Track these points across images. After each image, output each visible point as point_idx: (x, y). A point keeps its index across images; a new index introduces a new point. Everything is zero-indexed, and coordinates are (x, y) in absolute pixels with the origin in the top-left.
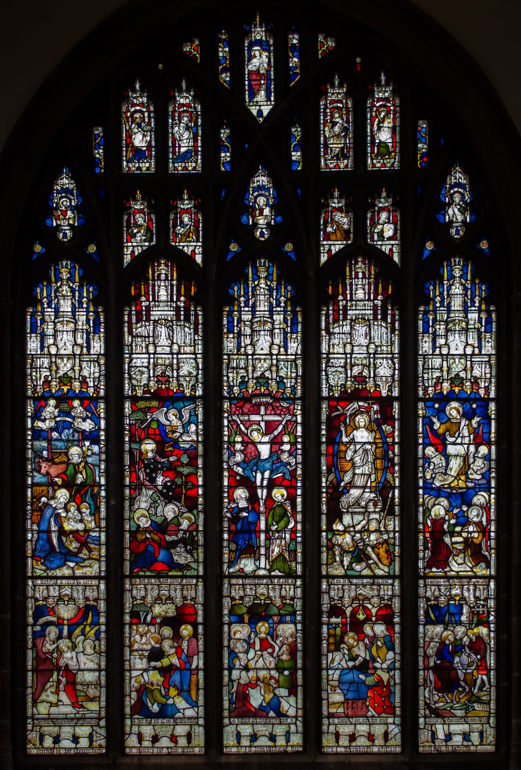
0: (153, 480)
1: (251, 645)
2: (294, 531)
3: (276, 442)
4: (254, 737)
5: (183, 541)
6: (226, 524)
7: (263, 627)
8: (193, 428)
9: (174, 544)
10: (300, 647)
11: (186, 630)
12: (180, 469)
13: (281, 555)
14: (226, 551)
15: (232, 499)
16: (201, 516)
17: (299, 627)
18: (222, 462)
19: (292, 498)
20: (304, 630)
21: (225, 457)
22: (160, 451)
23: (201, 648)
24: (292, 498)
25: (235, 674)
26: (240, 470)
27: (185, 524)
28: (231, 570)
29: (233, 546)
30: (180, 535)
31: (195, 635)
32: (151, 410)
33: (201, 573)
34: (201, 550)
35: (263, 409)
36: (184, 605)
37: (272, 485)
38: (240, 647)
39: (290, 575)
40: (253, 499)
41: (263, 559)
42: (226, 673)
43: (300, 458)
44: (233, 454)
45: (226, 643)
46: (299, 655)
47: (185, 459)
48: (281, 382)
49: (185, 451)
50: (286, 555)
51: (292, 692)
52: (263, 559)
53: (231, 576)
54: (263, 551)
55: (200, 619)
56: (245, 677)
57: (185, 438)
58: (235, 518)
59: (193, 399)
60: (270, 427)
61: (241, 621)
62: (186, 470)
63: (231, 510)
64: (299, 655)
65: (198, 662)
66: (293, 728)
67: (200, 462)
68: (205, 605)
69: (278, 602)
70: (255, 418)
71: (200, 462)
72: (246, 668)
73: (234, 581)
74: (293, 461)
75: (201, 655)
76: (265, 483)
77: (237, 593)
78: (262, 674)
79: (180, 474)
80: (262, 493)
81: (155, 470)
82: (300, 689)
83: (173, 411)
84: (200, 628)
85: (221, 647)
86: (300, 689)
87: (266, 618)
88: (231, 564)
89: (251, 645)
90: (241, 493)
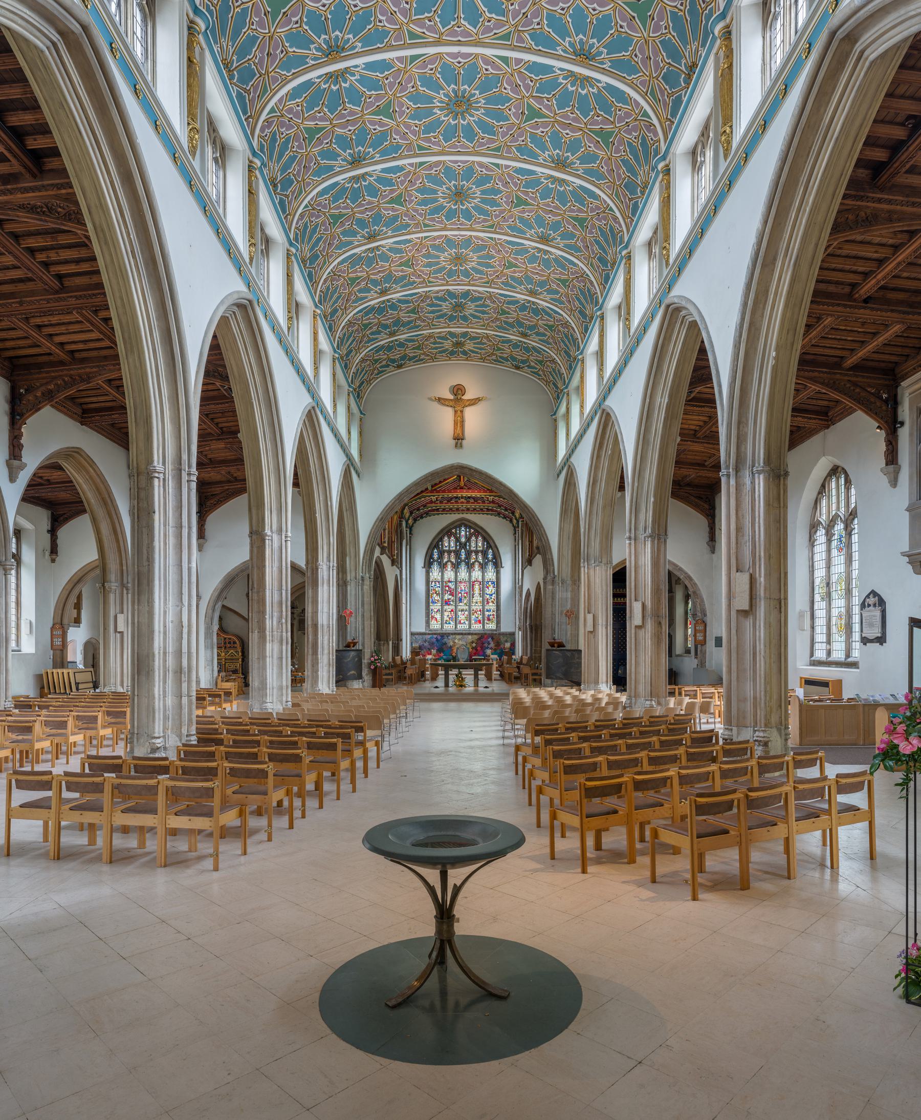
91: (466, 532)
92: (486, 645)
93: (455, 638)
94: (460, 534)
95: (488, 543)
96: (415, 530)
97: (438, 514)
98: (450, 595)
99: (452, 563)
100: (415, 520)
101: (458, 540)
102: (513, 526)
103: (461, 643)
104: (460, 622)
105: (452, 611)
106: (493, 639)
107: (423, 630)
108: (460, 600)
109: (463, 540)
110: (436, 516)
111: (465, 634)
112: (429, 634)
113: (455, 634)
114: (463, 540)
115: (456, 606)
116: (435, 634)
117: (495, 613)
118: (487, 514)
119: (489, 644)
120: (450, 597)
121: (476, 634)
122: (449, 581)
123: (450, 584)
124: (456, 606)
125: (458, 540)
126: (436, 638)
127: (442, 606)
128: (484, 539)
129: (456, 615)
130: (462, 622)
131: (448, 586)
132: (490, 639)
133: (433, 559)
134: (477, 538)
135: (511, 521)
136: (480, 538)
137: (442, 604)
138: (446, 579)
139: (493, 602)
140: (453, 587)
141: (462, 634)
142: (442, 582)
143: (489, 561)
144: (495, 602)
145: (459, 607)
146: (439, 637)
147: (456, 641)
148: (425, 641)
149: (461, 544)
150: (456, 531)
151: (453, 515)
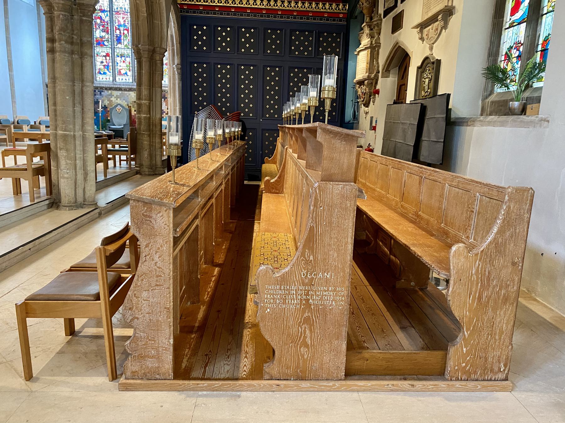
0: (99, 28)
1: (121, 62)
2: (129, 40)
3: (125, 21)
4: (122, 79)
5: (106, 40)
6: (115, 37)
7: (123, 58)
8: (107, 17)
9: (105, 41)
10: (131, 62)
12: (105, 26)
13: (126, 44)
14: (115, 43)
15: (116, 32)
16: (110, 36)
17: (131, 59)
18: (113, 25)
19: (128, 33)
20: (132, 59)
21: (114, 24)
22: (101, 22)
23: (111, 61)
24: (128, 33)
25: (118, 67)
26: (117, 27)
27: (107, 37)
28: (117, 46)
29: (117, 42)
30: (106, 39)
31: (110, 59)
32: (98, 13)
33: (110, 47)
34: (110, 42)
35: (121, 14)
36: (107, 53)
37: (124, 30)
38: (119, 62)
39: (128, 48)
40: (120, 33)
41: (123, 44)
42: (116, 67)
43: (130, 25)
44: (115, 23)
45: (116, 61)
46: (131, 64)
47: (106, 24)
48: (125, 9)
49: (106, 22)
50: (127, 44)
51: (130, 71)
52: (123, 44)
53: (116, 48)
54: (123, 43)
55: (111, 56)
56: (120, 68)
57: (106, 19)
58: (117, 37)
59: (107, 11)
60: (123, 18)
61: (119, 56)
62: (106, 26)
63: (116, 35)
64: (131, 64)
65: (111, 64)
66: (130, 78)
67: (109, 24)
68: (111, 53)
69: (126, 54)
70: (119, 16)
71: (109, 24)
72: (120, 66)
73: (117, 49)
74: (128, 25)
75: (111, 63)
76: (123, 30)
77: (118, 51)
78: (124, 67)
79: (105, 27)
80: (122, 32)
81: (100, 26)
82: (131, 71)
83: (103, 14)
84: (111, 58)
85: (115, 62)
86: (131, 71)
87: (124, 56)
88: (116, 45)
89: (121, 62)
90: (118, 32)
93: (111, 95)
98: (103, 31)
103: (119, 101)
104: (120, 72)
105: (107, 55)
108: (119, 40)
111: (125, 90)
113: (111, 89)
115: (113, 49)
120: (103, 34)
124: (113, 49)
129: (113, 61)
130: (123, 72)
131: (100, 18)
140: (107, 19)
141: (120, 89)
145: (117, 51)
147: (113, 99)
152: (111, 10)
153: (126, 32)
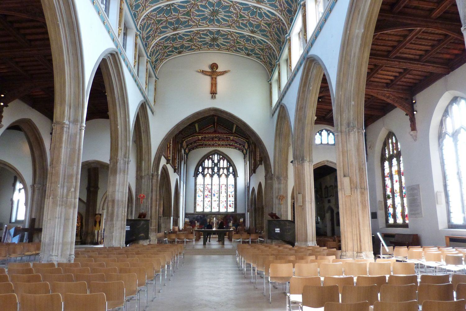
11: (209, 202)
91: (218, 157)
92: (229, 221)
94: (214, 158)
95: (230, 163)
96: (189, 155)
97: (203, 147)
99: (210, 174)
100: (190, 151)
101: (213, 161)
102: (244, 154)
106: (232, 217)
107: (192, 212)
109: (216, 161)
110: (201, 148)
112: (196, 214)
113: (211, 214)
114: (216, 161)
115: (211, 198)
116: (199, 214)
117: (234, 203)
118: (230, 148)
119: (230, 220)
121: (222, 214)
122: (208, 184)
123: (208, 186)
125: (213, 161)
126: (200, 217)
127: (204, 198)
128: (228, 161)
132: (231, 218)
133: (199, 172)
134: (224, 161)
135: (243, 152)
136: (225, 161)
137: (204, 197)
138: (206, 183)
139: (232, 196)
142: (204, 185)
143: (230, 173)
144: (234, 196)
146: (202, 216)
148: (194, 218)
149: (215, 163)
150: (212, 157)
151: (210, 148)
152: (212, 185)
153: (217, 192)
